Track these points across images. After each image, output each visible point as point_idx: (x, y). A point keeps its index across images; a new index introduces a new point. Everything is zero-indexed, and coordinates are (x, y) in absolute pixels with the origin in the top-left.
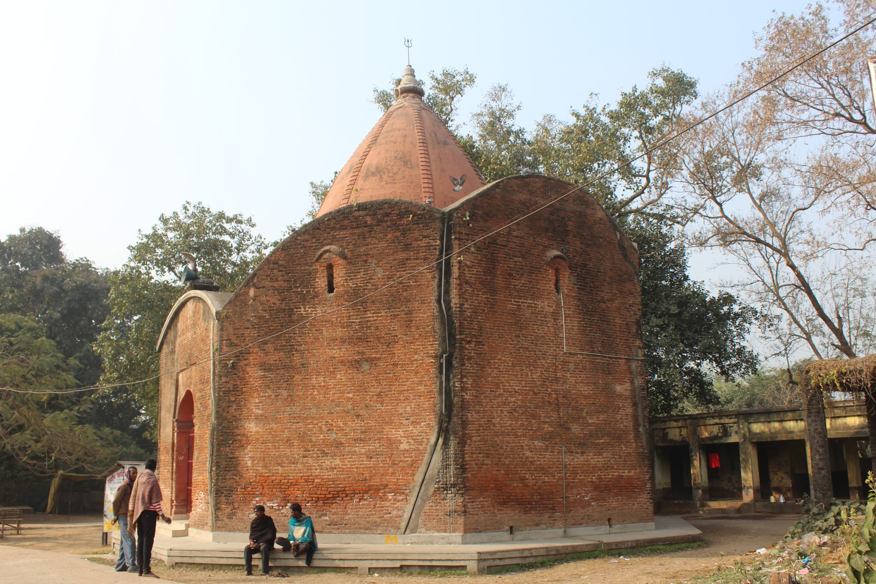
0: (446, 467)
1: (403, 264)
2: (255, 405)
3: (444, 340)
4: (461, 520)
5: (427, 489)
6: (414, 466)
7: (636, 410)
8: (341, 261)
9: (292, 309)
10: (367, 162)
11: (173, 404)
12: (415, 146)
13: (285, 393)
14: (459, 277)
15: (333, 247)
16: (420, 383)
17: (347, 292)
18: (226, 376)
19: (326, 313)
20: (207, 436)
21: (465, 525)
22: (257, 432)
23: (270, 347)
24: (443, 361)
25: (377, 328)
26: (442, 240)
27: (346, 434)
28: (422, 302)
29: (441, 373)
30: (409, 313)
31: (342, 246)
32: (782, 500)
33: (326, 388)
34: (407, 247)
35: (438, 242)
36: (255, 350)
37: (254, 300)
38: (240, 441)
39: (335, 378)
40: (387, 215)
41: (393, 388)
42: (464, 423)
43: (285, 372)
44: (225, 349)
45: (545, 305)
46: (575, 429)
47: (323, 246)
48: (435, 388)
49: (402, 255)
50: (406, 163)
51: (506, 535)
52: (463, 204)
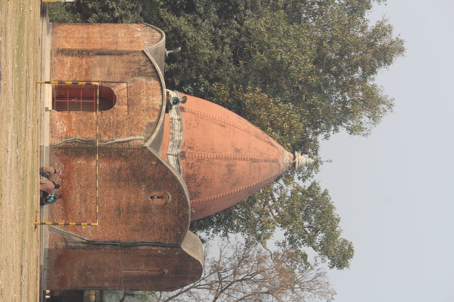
0: (75, 242)
1: (160, 228)
2: (103, 165)
3: (126, 244)
4: (53, 247)
5: (66, 235)
6: (75, 231)
7: (97, 287)
8: (164, 202)
9: (144, 181)
10: (238, 162)
11: (111, 80)
12: (246, 185)
13: (108, 178)
14: (151, 249)
15: (170, 200)
16: (109, 234)
17: (150, 205)
18: (117, 151)
19: (141, 196)
20: (91, 136)
21: (51, 249)
22: (92, 165)
23: (129, 171)
24: (117, 243)
25: (133, 217)
26: (168, 244)
27: (89, 204)
28: (142, 236)
29: (112, 242)
30: (138, 231)
31: (170, 203)
32: (47, 297)
33: (109, 196)
34: (167, 230)
35: (167, 243)
36: (128, 165)
37: (150, 164)
38: (88, 158)
39: (113, 199)
40: (182, 223)
41: (107, 223)
42: (91, 249)
43: (116, 178)
44: (129, 151)
45: (143, 267)
46: (89, 273)
47: (172, 195)
48: (106, 240)
49: (163, 229)
50: (234, 185)
51: (47, 256)
52: (184, 251)
